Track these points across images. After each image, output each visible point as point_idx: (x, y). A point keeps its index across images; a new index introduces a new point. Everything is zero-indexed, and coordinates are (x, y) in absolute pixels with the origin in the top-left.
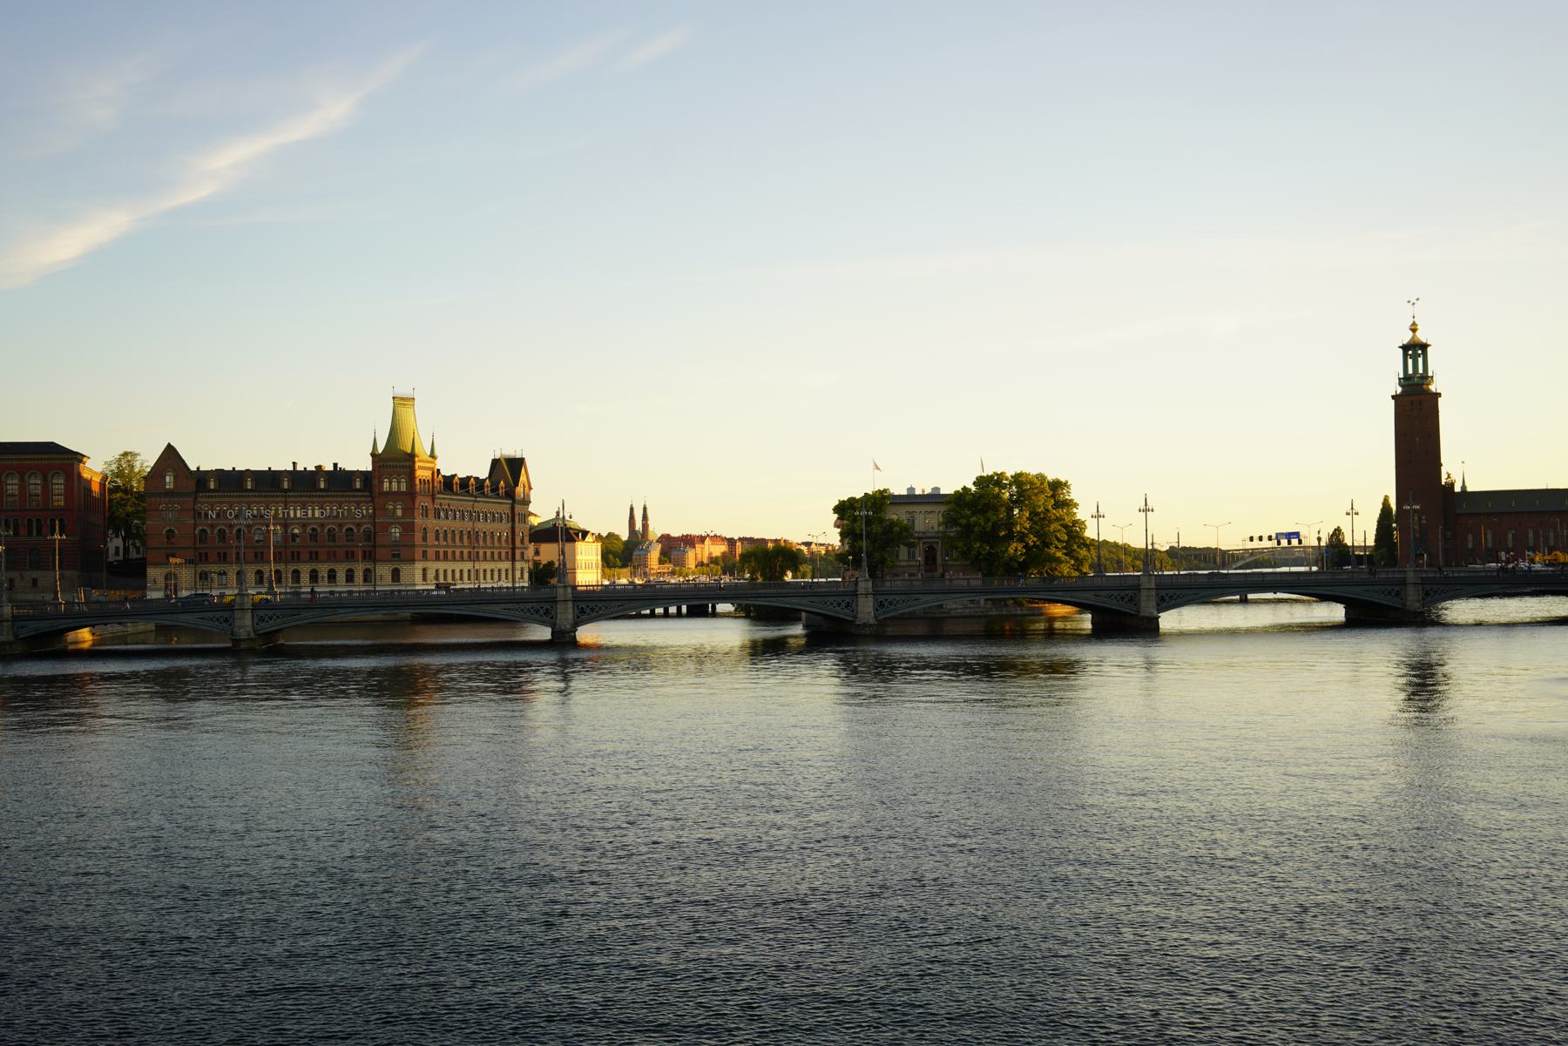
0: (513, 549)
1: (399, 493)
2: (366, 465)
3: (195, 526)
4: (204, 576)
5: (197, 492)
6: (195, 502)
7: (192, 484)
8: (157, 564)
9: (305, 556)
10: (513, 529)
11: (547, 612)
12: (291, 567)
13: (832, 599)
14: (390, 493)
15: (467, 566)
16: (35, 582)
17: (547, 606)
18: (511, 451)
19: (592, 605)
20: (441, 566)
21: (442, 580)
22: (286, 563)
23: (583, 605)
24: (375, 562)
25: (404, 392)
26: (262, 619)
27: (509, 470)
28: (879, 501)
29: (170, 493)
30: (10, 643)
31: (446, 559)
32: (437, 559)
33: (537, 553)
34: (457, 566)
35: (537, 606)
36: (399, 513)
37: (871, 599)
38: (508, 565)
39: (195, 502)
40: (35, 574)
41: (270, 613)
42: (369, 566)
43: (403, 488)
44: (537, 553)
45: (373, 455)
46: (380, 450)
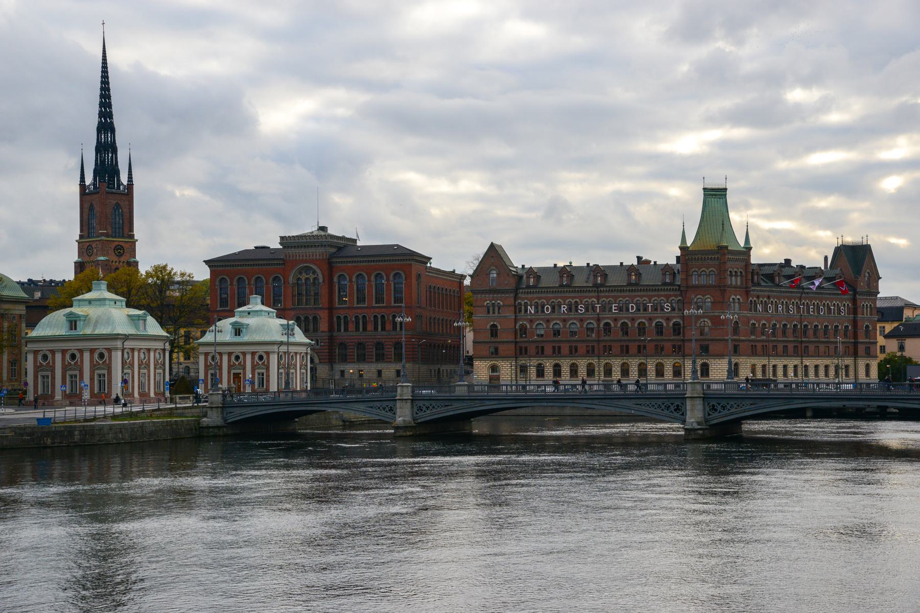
0: (856, 344)
3: (516, 320)
4: (524, 369)
6: (515, 299)
7: (511, 283)
8: (482, 358)
9: (616, 349)
10: (855, 323)
11: (677, 409)
12: (603, 362)
14: (697, 287)
15: (792, 362)
16: (380, 373)
17: (677, 402)
19: (724, 402)
20: (759, 362)
21: (759, 376)
22: (599, 357)
23: (714, 402)
24: (684, 356)
25: (715, 182)
26: (420, 409)
27: (622, 263)
30: (218, 427)
31: (765, 353)
32: (754, 353)
33: (902, 348)
34: (780, 363)
35: (667, 403)
38: (849, 361)
40: (380, 366)
41: (427, 403)
42: (678, 360)
44: (902, 348)
45: (683, 248)
46: (689, 243)
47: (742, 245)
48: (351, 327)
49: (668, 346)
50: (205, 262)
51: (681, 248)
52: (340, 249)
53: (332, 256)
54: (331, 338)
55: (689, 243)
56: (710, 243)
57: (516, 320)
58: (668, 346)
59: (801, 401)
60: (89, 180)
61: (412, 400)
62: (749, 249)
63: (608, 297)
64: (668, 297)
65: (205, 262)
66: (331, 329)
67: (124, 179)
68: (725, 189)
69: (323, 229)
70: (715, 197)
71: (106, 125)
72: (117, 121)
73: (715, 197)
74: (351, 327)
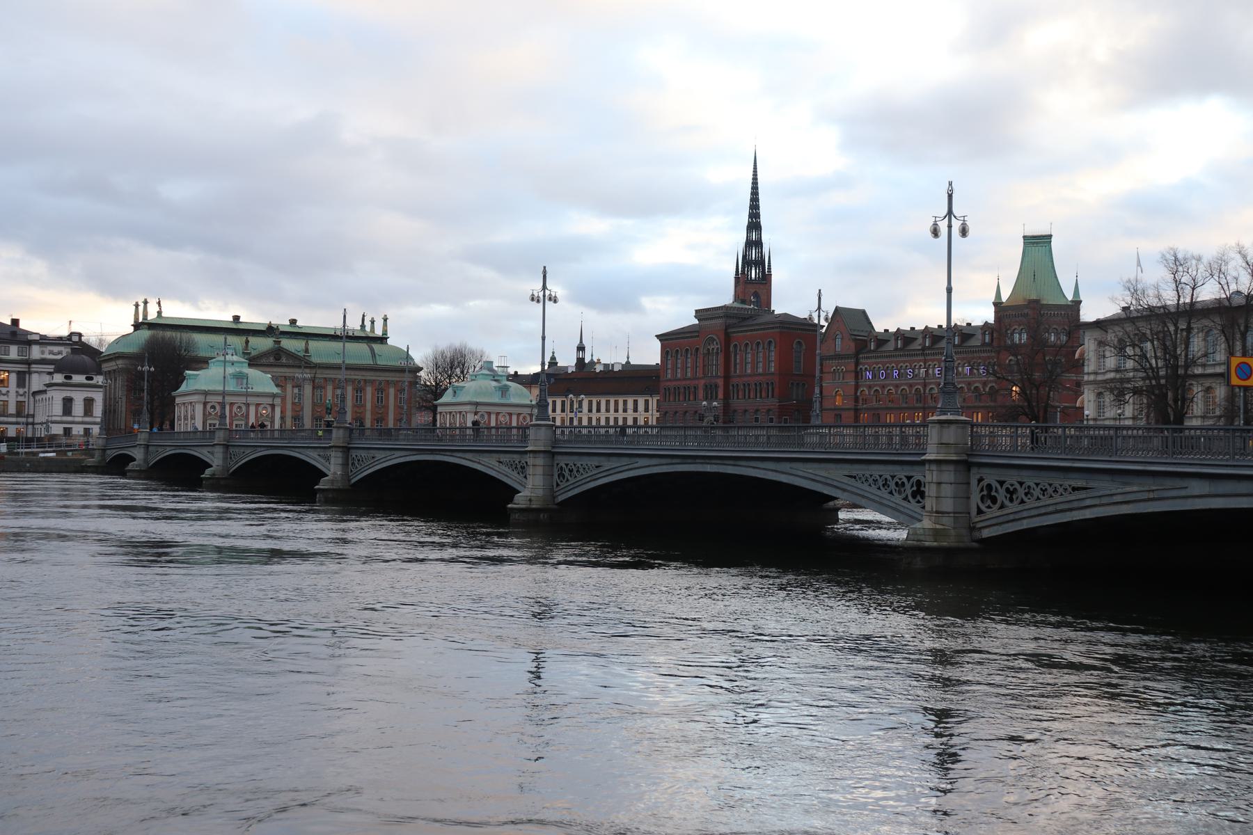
3: (857, 387)
6: (857, 364)
29: (838, 357)
39: (857, 364)
45: (997, 305)
46: (1004, 298)
47: (1070, 297)
50: (657, 336)
51: (995, 304)
52: (744, 319)
55: (1004, 298)
57: (857, 387)
59: (654, 461)
62: (1077, 303)
63: (933, 360)
65: (657, 336)
66: (727, 396)
68: (1050, 236)
70: (1037, 244)
71: (754, 225)
72: (764, 221)
73: (1037, 244)
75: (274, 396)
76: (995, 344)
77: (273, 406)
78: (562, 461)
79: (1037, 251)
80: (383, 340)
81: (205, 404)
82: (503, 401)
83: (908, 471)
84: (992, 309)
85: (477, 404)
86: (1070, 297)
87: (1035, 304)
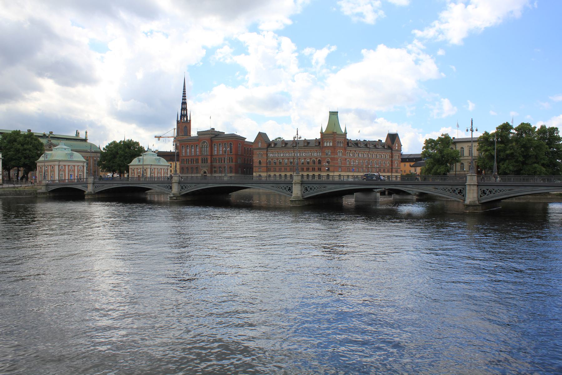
1: (330, 146)
2: (319, 137)
3: (267, 159)
5: (267, 148)
6: (267, 151)
13: (282, 185)
14: (327, 147)
18: (393, 131)
23: (182, 185)
28: (446, 141)
29: (260, 149)
36: (330, 153)
37: (475, 188)
39: (267, 151)
43: (331, 145)
45: (322, 133)
46: (324, 131)
47: (344, 132)
48: (218, 161)
49: (316, 168)
52: (216, 135)
53: (213, 137)
54: (212, 165)
55: (324, 131)
56: (330, 131)
57: (267, 159)
58: (316, 168)
60: (179, 119)
61: (93, 184)
62: (346, 133)
64: (316, 150)
66: (211, 162)
67: (189, 119)
69: (213, 129)
70: (334, 115)
74: (218, 161)
75: (84, 162)
76: (321, 145)
77: (83, 166)
78: (96, 185)
79: (333, 116)
80: (85, 140)
81: (59, 166)
82: (159, 164)
83: (287, 185)
84: (320, 134)
85: (151, 165)
86: (344, 132)
87: (334, 133)
